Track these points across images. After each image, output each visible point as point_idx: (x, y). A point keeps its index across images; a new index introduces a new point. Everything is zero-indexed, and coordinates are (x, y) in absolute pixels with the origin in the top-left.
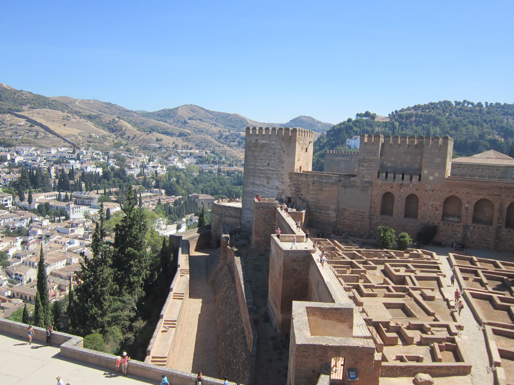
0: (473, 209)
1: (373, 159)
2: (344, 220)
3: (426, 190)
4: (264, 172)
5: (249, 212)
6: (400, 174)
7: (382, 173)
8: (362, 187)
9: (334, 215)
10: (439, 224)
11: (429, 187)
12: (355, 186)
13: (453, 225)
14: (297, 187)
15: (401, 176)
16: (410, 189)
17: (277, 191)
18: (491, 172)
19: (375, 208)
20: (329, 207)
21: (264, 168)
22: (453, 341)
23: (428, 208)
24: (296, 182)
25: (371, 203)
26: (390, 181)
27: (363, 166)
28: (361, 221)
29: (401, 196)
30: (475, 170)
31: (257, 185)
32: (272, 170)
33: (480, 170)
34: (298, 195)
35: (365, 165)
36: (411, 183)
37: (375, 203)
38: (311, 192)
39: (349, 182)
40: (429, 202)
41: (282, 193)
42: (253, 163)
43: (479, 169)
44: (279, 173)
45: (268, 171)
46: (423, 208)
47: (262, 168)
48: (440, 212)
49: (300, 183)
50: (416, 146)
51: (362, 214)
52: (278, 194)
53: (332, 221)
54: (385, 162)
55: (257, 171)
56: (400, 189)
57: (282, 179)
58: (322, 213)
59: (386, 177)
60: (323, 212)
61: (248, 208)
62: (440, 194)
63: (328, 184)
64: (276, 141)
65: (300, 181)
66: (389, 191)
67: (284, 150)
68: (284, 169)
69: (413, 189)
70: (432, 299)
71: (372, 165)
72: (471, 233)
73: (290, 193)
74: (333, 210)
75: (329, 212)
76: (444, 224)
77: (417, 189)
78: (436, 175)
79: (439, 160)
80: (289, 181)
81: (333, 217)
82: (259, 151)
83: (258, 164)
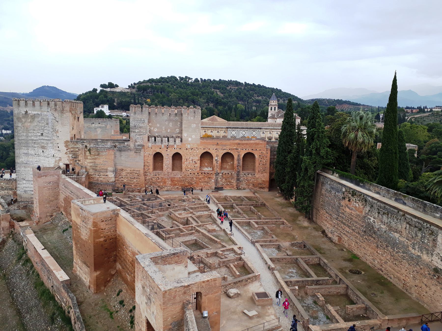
0: (220, 160)
2: (122, 179)
4: (38, 142)
5: (24, 182)
6: (166, 137)
7: (151, 137)
8: (136, 149)
9: (113, 176)
10: (198, 173)
11: (189, 147)
13: (208, 173)
14: (74, 154)
15: (167, 139)
17: (54, 159)
18: (218, 132)
20: (107, 169)
21: (38, 138)
22: (240, 259)
24: (72, 150)
26: (158, 143)
28: (137, 178)
30: (206, 131)
31: (32, 155)
32: (46, 140)
33: (210, 131)
34: (76, 161)
35: (137, 131)
36: (175, 144)
37: (148, 163)
38: (89, 157)
39: (124, 146)
41: (60, 160)
42: (25, 134)
43: (209, 130)
44: (54, 142)
45: (42, 141)
47: (36, 138)
48: (198, 165)
49: (77, 150)
50: (176, 114)
51: (138, 172)
52: (56, 162)
53: (111, 181)
54: (152, 128)
55: (30, 142)
56: (167, 150)
57: (58, 147)
58: (101, 175)
59: (155, 140)
60: (102, 174)
61: (23, 179)
62: (197, 151)
63: (104, 149)
64: (48, 112)
67: (57, 120)
68: (60, 138)
70: (214, 230)
72: (220, 178)
73: (68, 160)
74: (111, 171)
75: (107, 174)
76: (202, 174)
78: (193, 137)
79: (195, 125)
80: (65, 149)
81: (112, 177)
82: (30, 122)
83: (30, 135)
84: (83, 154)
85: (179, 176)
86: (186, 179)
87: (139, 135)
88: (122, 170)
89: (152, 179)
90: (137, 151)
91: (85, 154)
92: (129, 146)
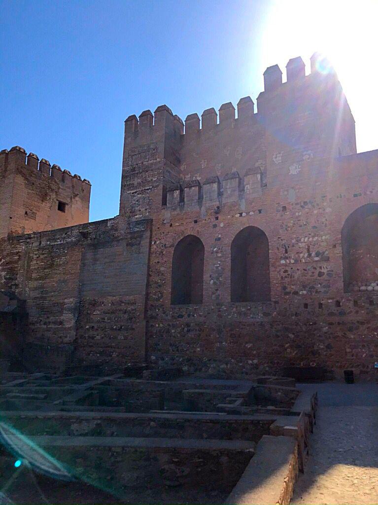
1: (152, 164)
2: (91, 333)
3: (284, 208)
6: (213, 182)
10: (338, 304)
12: (116, 238)
15: (215, 185)
16: (241, 214)
19: (160, 286)
23: (296, 261)
24: (8, 259)
25: (149, 275)
27: (131, 186)
28: (127, 329)
29: (219, 239)
35: (136, 181)
36: (241, 197)
37: (159, 273)
40: (298, 241)
46: (283, 262)
53: (66, 340)
56: (216, 222)
60: (52, 318)
65: (18, 253)
66: (189, 232)
69: (248, 213)
71: (149, 179)
77: (260, 211)
84: (26, 268)
85: (260, 318)
86: (287, 329)
87: (142, 192)
88: (94, 305)
89: (168, 331)
90: (133, 241)
91: (29, 266)
92: (116, 230)
